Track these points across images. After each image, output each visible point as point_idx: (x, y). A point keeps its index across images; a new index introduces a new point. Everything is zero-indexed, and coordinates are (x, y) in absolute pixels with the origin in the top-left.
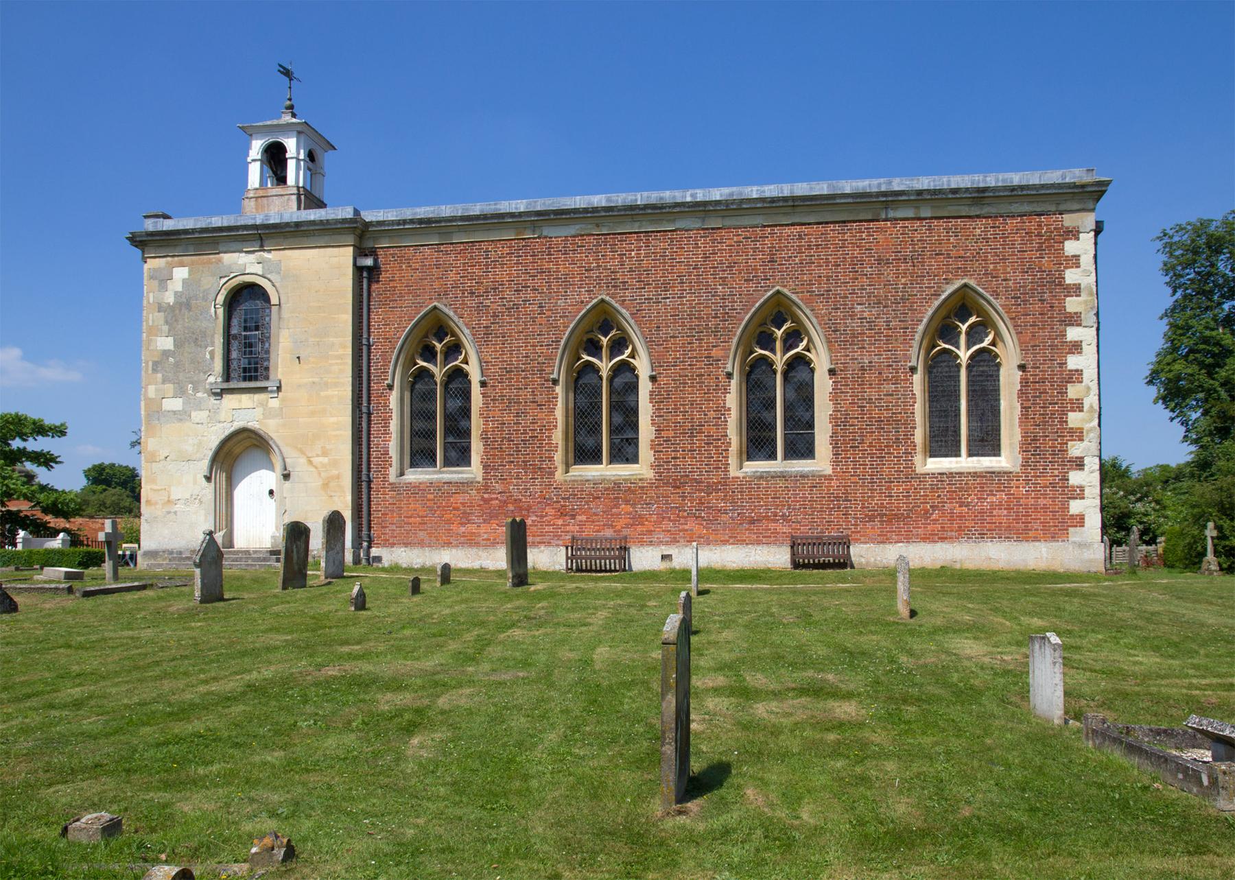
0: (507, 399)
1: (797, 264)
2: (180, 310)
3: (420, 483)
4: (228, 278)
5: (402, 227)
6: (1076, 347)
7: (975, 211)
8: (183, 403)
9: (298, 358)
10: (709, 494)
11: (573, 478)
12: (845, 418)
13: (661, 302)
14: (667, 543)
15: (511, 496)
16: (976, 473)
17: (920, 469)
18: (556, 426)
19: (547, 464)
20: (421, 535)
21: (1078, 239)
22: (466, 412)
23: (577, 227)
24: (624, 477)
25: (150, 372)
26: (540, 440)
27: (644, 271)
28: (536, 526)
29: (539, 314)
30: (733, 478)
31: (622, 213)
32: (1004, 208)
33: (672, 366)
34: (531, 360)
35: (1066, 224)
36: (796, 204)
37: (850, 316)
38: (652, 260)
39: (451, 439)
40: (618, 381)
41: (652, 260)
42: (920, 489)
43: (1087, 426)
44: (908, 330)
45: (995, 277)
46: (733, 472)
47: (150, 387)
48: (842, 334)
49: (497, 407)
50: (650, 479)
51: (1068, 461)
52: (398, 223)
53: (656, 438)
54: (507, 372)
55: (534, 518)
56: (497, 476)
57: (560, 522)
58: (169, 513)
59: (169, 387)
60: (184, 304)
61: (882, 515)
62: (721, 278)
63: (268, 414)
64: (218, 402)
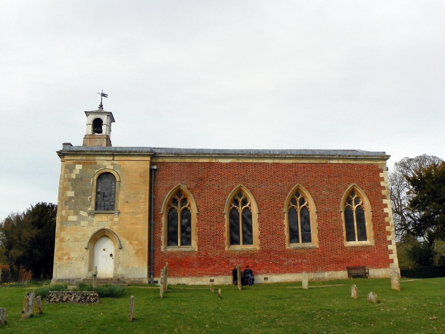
0: (207, 220)
1: (303, 176)
2: (78, 181)
3: (173, 252)
4: (99, 170)
5: (168, 155)
8: (77, 218)
9: (127, 202)
10: (279, 255)
11: (232, 250)
12: (322, 228)
13: (260, 187)
14: (265, 274)
15: (209, 257)
16: (362, 246)
17: (345, 246)
18: (225, 230)
21: (383, 172)
22: (189, 224)
23: (231, 160)
24: (249, 249)
25: (64, 205)
26: (219, 236)
27: (254, 176)
28: (218, 268)
29: (218, 190)
30: (287, 249)
31: (247, 156)
33: (265, 210)
34: (215, 206)
36: (303, 157)
37: (321, 194)
38: (257, 173)
39: (183, 235)
41: (257, 173)
43: (391, 230)
46: (287, 247)
47: (63, 211)
48: (319, 200)
49: (203, 223)
50: (259, 250)
51: (387, 242)
53: (260, 235)
54: (207, 210)
55: (217, 265)
56: (203, 249)
58: (68, 263)
59: (72, 211)
60: (80, 179)
62: (280, 180)
64: (92, 218)
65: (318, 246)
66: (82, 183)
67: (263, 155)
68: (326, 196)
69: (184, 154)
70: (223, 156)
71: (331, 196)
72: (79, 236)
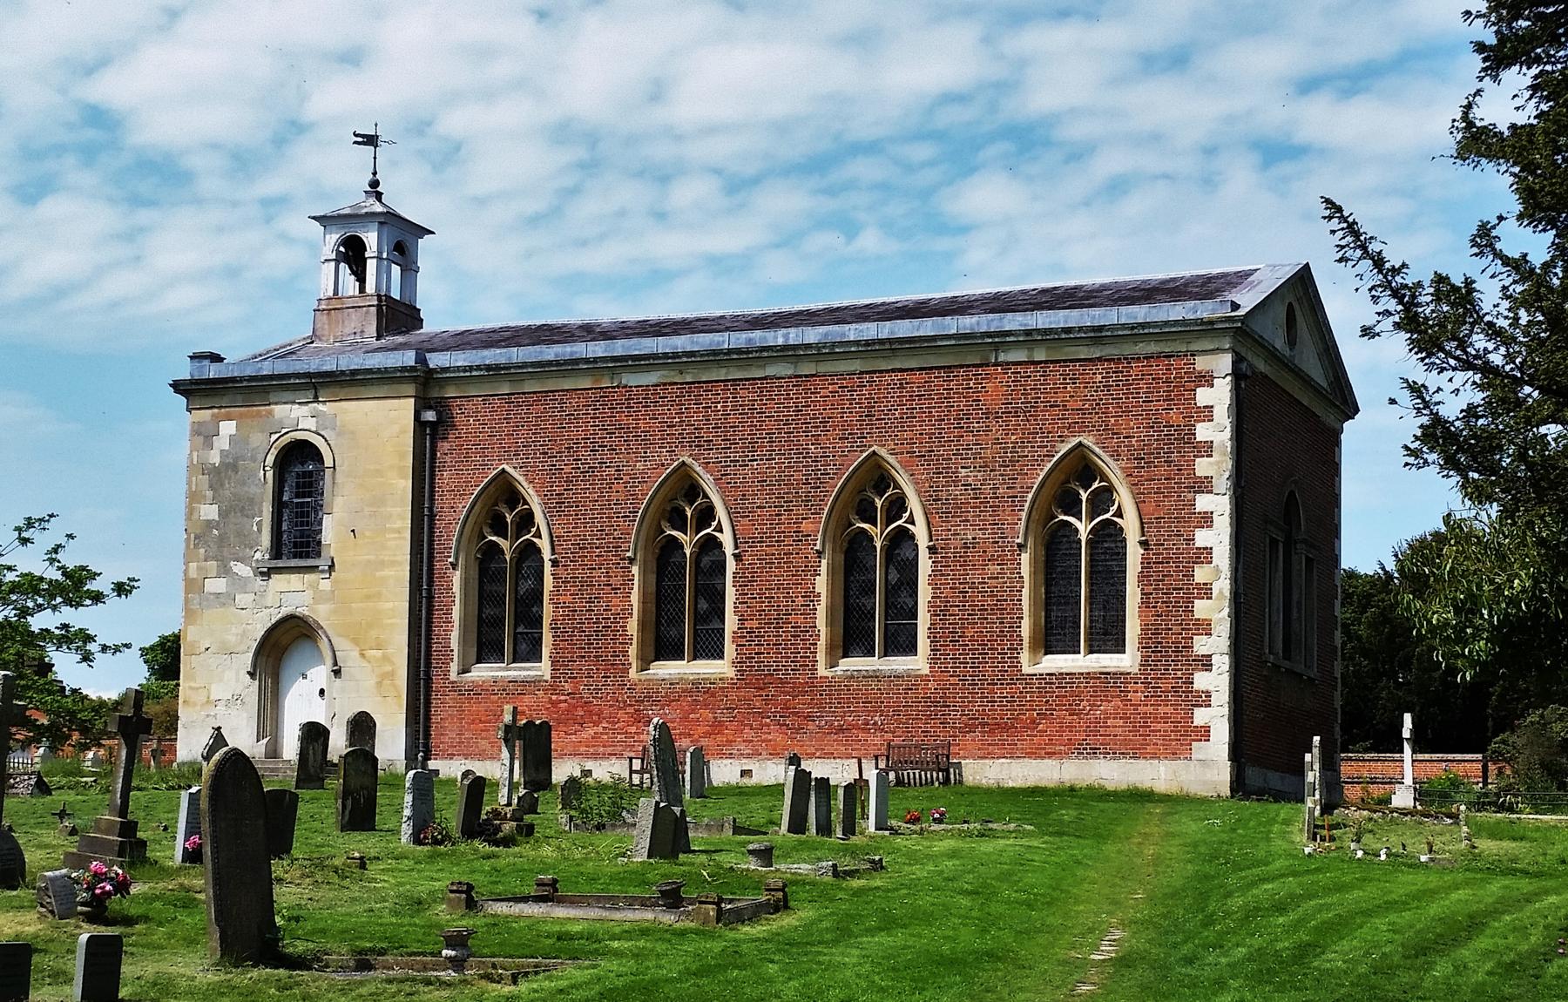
3: (483, 682)
4: (278, 435)
5: (468, 374)
6: (1207, 520)
7: (1096, 353)
9: (353, 531)
11: (648, 677)
12: (945, 606)
13: (747, 465)
14: (749, 756)
19: (620, 660)
20: (484, 744)
25: (192, 546)
27: (731, 427)
28: (607, 734)
29: (616, 479)
31: (706, 358)
32: (1128, 349)
34: (606, 535)
35: (1198, 368)
37: (953, 481)
40: (706, 560)
42: (1027, 692)
43: (1215, 617)
44: (1015, 500)
45: (1116, 434)
50: (732, 679)
51: (1193, 660)
52: (465, 369)
53: (739, 629)
54: (580, 548)
57: (633, 730)
58: (208, 716)
61: (983, 725)
62: (813, 436)
63: (318, 598)
64: (265, 583)
65: (926, 671)
66: (238, 477)
67: (756, 352)
68: (972, 490)
69: (514, 367)
70: (630, 363)
71: (987, 489)
72: (232, 637)
